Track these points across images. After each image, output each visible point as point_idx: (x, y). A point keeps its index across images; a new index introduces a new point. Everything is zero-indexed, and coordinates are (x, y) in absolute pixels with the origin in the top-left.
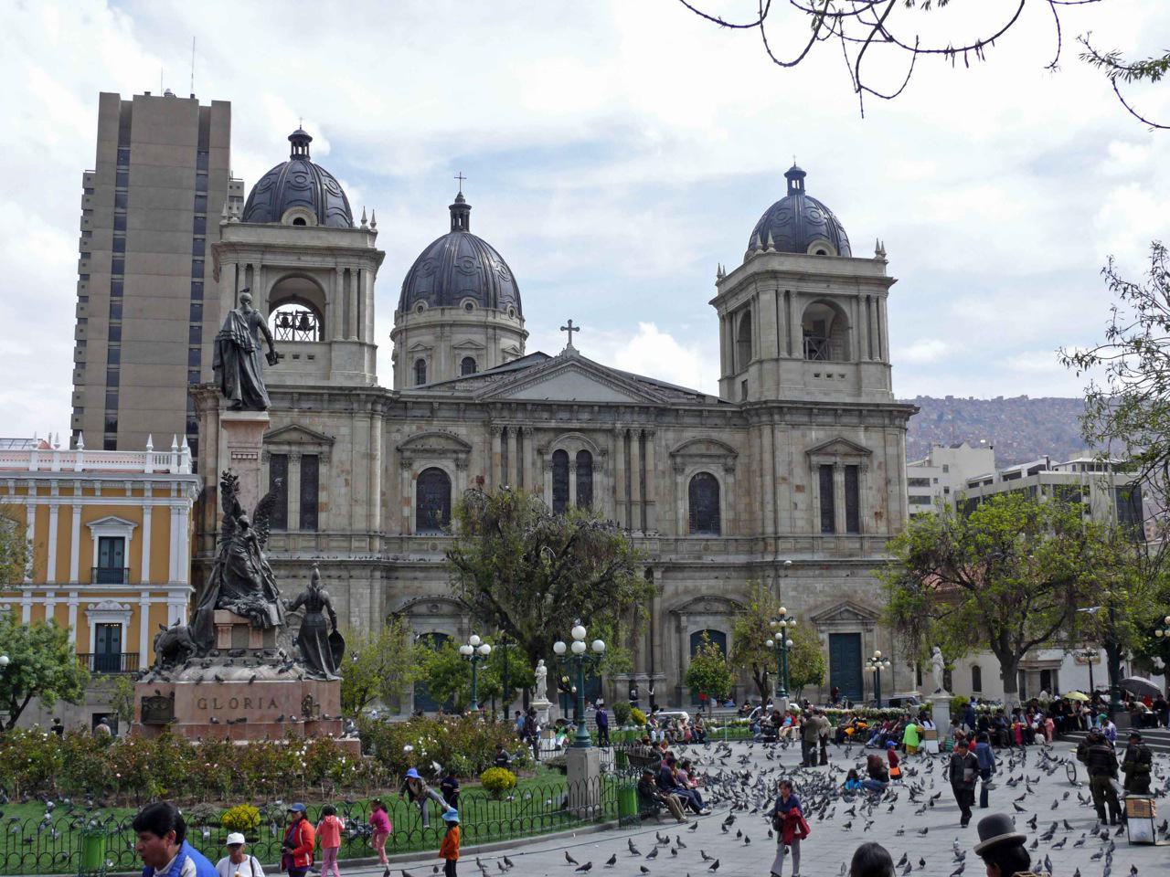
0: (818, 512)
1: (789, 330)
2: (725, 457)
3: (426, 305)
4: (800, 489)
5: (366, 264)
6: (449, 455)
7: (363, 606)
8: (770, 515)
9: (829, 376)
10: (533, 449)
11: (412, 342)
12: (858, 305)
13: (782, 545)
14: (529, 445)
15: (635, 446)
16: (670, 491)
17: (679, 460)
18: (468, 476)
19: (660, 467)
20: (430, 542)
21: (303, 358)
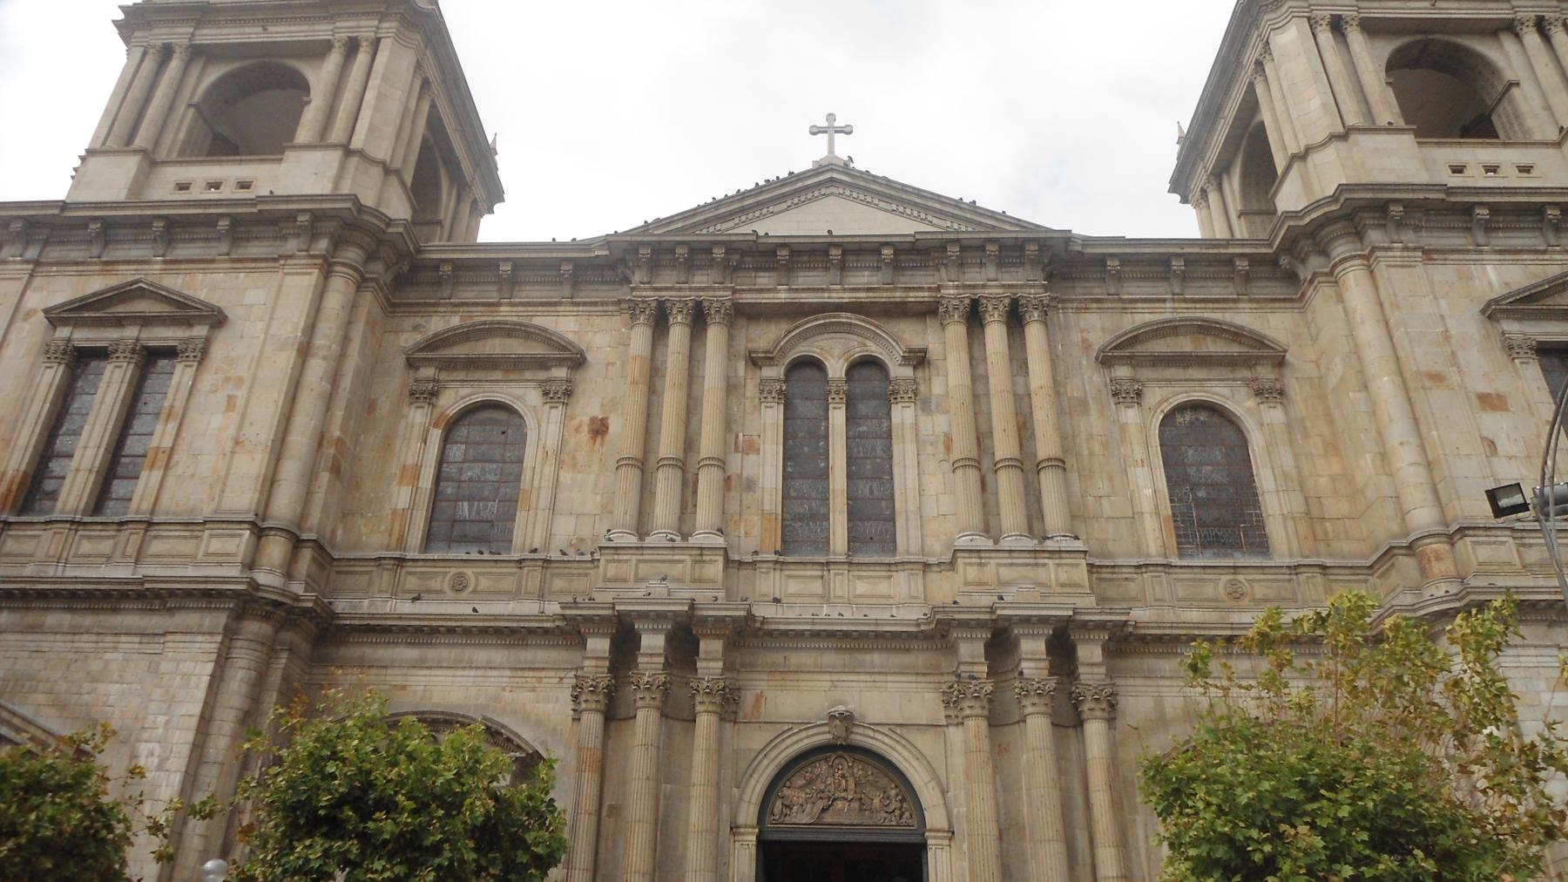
2: (1248, 362)
6: (528, 375)
7: (181, 710)
10: (731, 355)
12: (1518, 36)
15: (995, 334)
16: (1105, 446)
18: (567, 419)
20: (453, 571)
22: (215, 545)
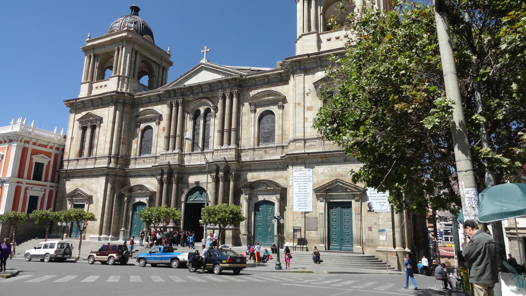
9: (338, 38)
16: (247, 123)
18: (158, 129)
21: (103, 87)
22: (104, 160)
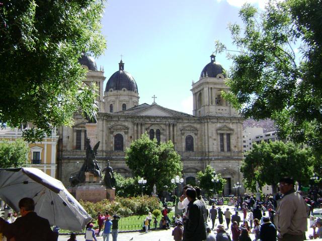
0: (219, 146)
1: (212, 98)
3: (113, 90)
4: (215, 140)
5: (101, 80)
8: (207, 146)
9: (222, 110)
11: (109, 100)
13: (210, 154)
14: (143, 128)
17: (183, 132)
19: (178, 134)
